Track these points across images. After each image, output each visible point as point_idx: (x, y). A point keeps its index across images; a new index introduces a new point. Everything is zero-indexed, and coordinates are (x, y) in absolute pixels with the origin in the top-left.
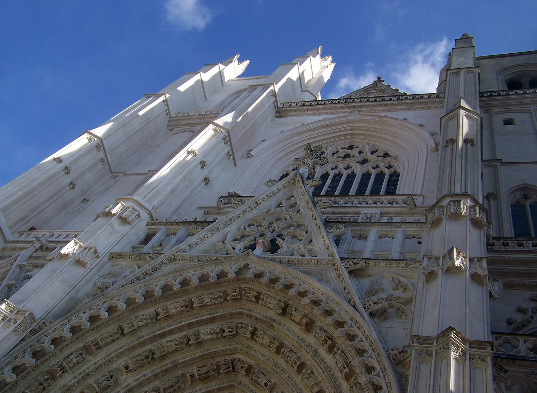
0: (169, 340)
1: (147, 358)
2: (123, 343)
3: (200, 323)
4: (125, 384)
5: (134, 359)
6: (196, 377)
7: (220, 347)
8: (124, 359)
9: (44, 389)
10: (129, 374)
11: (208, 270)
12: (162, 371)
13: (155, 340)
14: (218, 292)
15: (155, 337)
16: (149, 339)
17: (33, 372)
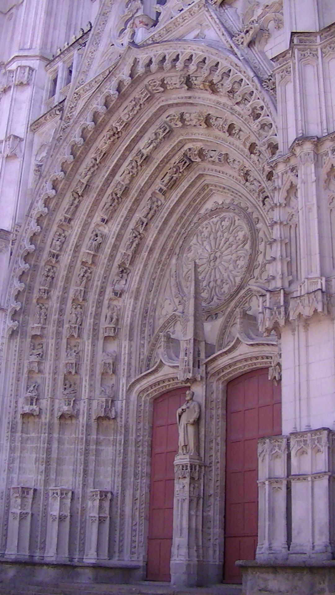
0: (120, 174)
1: (113, 200)
2: (87, 203)
3: (136, 140)
4: (112, 233)
5: (104, 210)
6: (165, 189)
7: (166, 149)
8: (97, 214)
9: (53, 278)
10: (110, 224)
11: (107, 90)
12: (134, 203)
13: (109, 182)
14: (128, 103)
15: (107, 179)
16: (104, 185)
17: (36, 272)
